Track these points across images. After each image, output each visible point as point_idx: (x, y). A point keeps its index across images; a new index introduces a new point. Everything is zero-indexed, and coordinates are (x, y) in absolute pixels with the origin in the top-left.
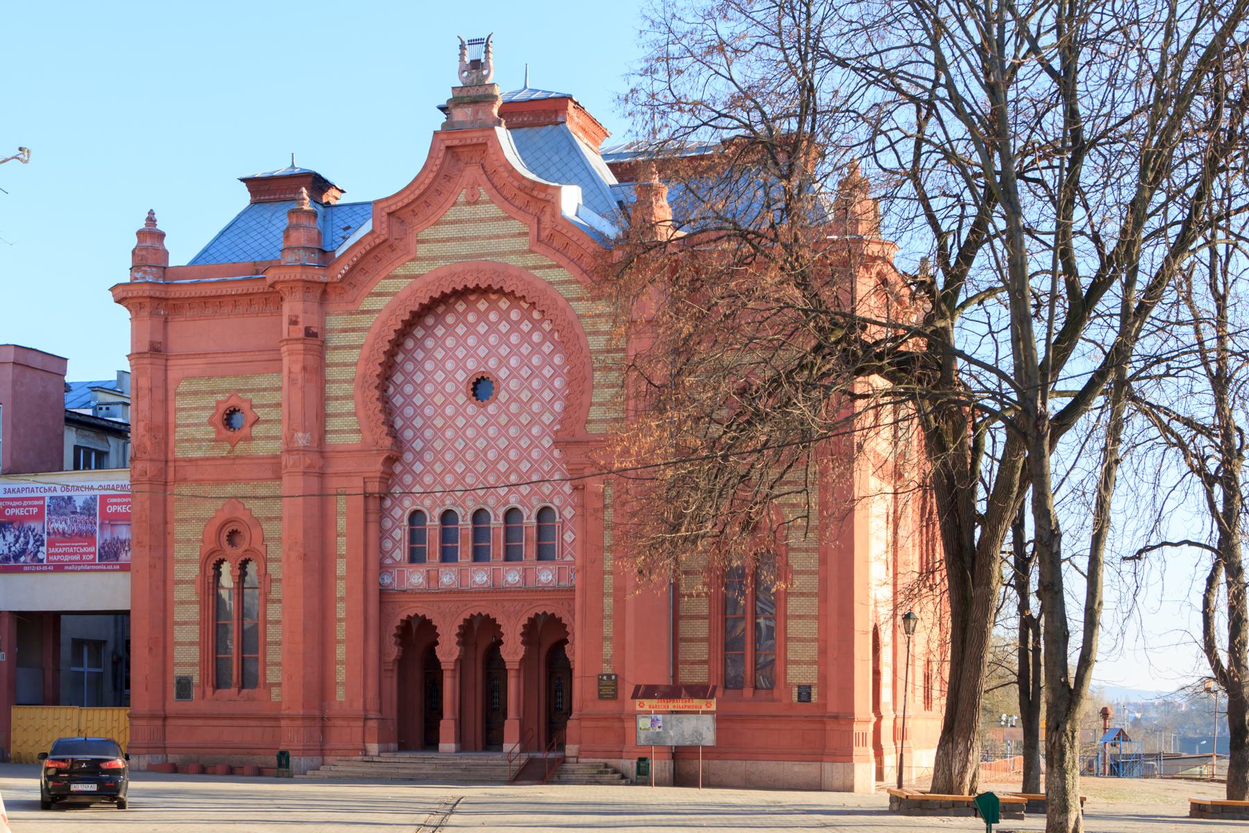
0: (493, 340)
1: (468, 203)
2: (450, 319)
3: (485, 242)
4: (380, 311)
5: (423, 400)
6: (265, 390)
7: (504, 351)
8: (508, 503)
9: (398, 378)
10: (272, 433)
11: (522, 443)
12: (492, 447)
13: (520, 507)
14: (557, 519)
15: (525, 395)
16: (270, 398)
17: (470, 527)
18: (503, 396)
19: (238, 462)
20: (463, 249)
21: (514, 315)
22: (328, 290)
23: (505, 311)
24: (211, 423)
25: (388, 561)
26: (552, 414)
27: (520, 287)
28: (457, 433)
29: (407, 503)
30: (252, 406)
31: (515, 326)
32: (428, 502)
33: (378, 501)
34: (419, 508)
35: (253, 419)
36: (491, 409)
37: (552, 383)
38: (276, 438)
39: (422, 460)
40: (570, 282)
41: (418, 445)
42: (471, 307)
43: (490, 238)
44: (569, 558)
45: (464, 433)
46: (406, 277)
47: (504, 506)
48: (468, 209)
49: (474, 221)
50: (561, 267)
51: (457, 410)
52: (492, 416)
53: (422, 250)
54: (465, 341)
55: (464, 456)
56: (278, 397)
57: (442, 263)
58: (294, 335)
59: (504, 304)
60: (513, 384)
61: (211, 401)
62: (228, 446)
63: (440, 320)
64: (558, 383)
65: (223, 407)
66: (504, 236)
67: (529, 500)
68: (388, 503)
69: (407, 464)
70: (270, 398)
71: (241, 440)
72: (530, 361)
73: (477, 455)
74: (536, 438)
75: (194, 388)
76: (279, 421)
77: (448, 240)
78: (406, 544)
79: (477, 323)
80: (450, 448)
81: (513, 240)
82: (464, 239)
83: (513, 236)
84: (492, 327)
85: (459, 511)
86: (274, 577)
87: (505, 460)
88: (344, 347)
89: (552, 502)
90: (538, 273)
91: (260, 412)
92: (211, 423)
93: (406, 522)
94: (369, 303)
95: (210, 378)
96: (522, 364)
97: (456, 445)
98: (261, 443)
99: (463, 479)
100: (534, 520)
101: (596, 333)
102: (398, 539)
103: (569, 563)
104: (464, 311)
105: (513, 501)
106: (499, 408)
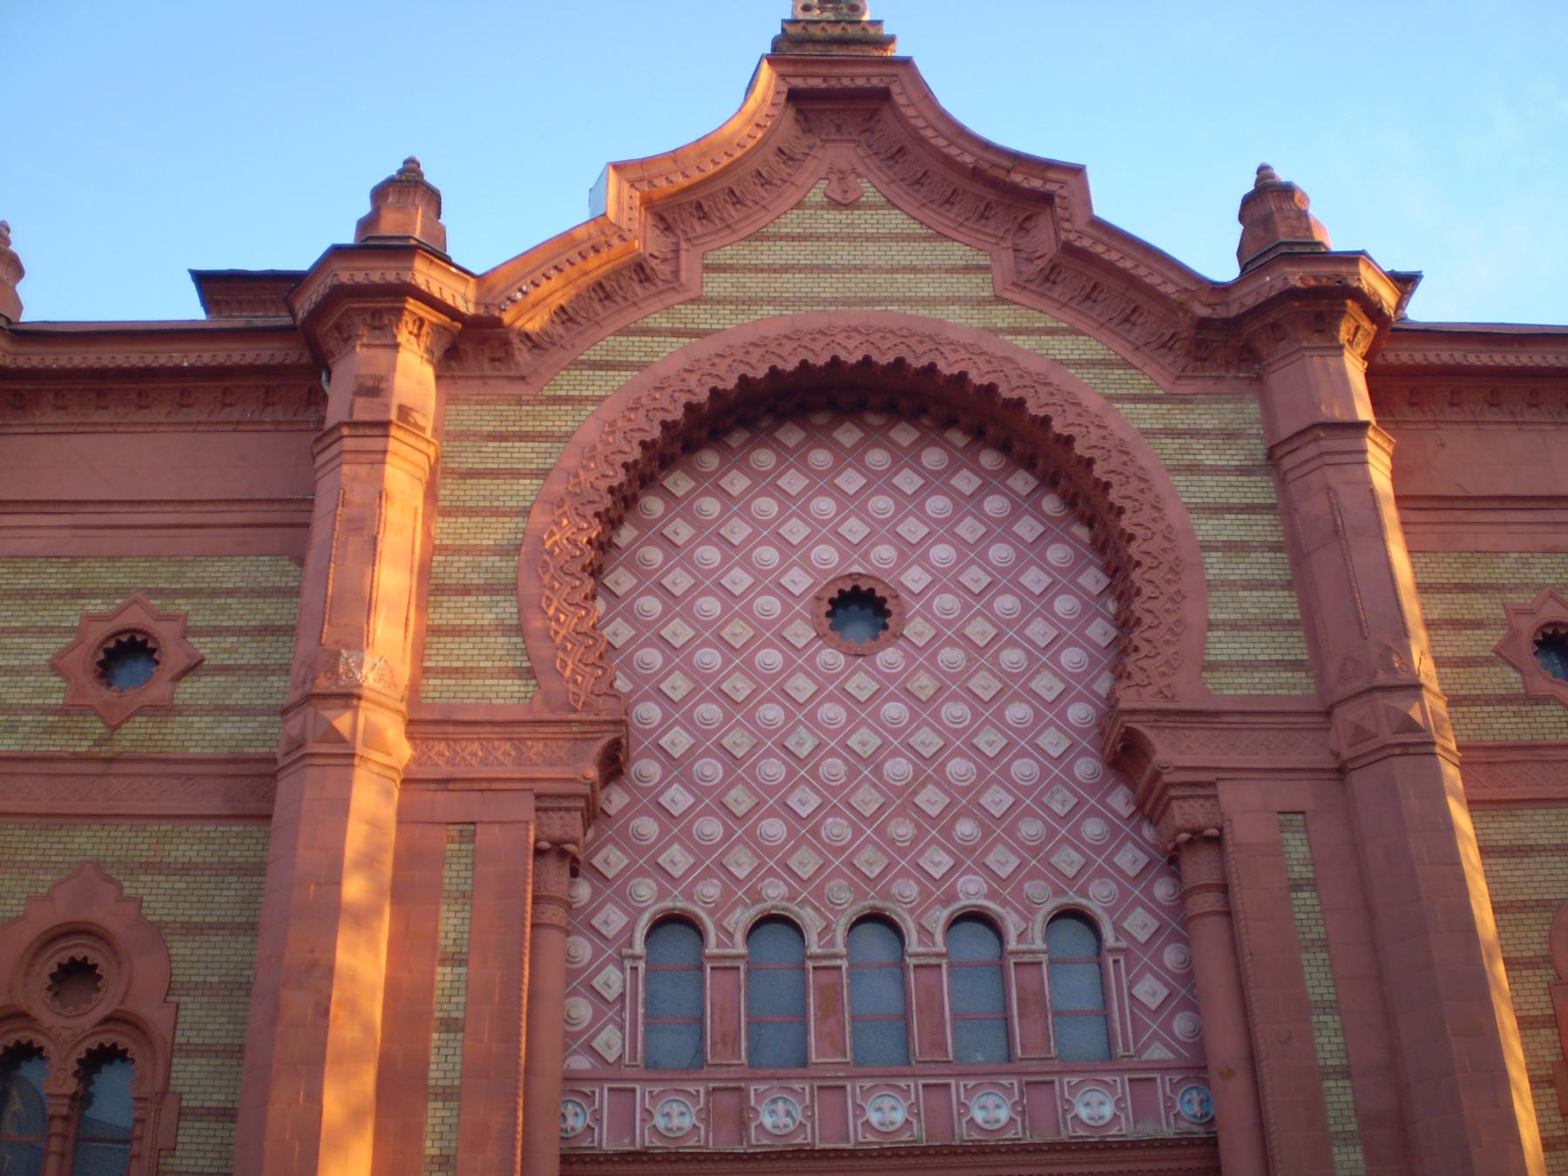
0: (881, 504)
1: (836, 205)
2: (764, 458)
3: (882, 279)
4: (599, 400)
5: (689, 633)
6: (230, 593)
7: (913, 529)
8: (951, 896)
9: (621, 580)
10: (237, 698)
11: (980, 742)
12: (896, 753)
13: (993, 906)
14: (1109, 939)
15: (979, 631)
16: (241, 613)
17: (844, 964)
18: (917, 630)
19: (118, 768)
20: (827, 286)
21: (933, 458)
22: (462, 346)
23: (906, 451)
24: (55, 668)
25: (581, 1063)
26: (1056, 674)
27: (984, 368)
28: (789, 715)
29: (645, 890)
30: (187, 631)
31: (936, 482)
32: (711, 890)
33: (566, 871)
34: (681, 904)
35: (184, 663)
36: (890, 656)
37: (1049, 606)
38: (246, 711)
39: (688, 782)
40: (1107, 364)
41: (678, 740)
42: (819, 436)
43: (893, 270)
44: (1157, 1053)
45: (812, 716)
46: (675, 333)
47: (945, 904)
48: (833, 215)
49: (852, 238)
50: (1084, 334)
51: (789, 662)
52: (891, 678)
53: (716, 285)
54: (805, 507)
55: (814, 772)
56: (271, 611)
57: (769, 311)
58: (359, 416)
59: (904, 435)
60: (947, 603)
61: (70, 615)
62: (98, 728)
63: (735, 459)
64: (1064, 605)
65: (106, 629)
66: (929, 270)
67: (1017, 893)
68: (583, 891)
69: (645, 792)
70: (241, 613)
71: (140, 711)
72: (983, 555)
73: (853, 773)
74: (1023, 733)
75: (24, 582)
76: (264, 670)
77: (785, 269)
78: (641, 1010)
79: (837, 468)
80: (769, 754)
81: (952, 278)
82: (827, 269)
83: (953, 270)
84: (878, 482)
85: (809, 918)
86: (189, 1102)
88: (494, 474)
89: (1088, 898)
90: (1022, 342)
91: (205, 647)
92: (55, 668)
93: (639, 947)
94: (567, 383)
95: (74, 559)
96: (962, 562)
97: (791, 743)
98: (198, 722)
99: (815, 832)
100: (1039, 944)
101: (1194, 469)
102: (611, 995)
103: (1164, 1068)
104: (799, 445)
105: (972, 891)
106: (909, 659)
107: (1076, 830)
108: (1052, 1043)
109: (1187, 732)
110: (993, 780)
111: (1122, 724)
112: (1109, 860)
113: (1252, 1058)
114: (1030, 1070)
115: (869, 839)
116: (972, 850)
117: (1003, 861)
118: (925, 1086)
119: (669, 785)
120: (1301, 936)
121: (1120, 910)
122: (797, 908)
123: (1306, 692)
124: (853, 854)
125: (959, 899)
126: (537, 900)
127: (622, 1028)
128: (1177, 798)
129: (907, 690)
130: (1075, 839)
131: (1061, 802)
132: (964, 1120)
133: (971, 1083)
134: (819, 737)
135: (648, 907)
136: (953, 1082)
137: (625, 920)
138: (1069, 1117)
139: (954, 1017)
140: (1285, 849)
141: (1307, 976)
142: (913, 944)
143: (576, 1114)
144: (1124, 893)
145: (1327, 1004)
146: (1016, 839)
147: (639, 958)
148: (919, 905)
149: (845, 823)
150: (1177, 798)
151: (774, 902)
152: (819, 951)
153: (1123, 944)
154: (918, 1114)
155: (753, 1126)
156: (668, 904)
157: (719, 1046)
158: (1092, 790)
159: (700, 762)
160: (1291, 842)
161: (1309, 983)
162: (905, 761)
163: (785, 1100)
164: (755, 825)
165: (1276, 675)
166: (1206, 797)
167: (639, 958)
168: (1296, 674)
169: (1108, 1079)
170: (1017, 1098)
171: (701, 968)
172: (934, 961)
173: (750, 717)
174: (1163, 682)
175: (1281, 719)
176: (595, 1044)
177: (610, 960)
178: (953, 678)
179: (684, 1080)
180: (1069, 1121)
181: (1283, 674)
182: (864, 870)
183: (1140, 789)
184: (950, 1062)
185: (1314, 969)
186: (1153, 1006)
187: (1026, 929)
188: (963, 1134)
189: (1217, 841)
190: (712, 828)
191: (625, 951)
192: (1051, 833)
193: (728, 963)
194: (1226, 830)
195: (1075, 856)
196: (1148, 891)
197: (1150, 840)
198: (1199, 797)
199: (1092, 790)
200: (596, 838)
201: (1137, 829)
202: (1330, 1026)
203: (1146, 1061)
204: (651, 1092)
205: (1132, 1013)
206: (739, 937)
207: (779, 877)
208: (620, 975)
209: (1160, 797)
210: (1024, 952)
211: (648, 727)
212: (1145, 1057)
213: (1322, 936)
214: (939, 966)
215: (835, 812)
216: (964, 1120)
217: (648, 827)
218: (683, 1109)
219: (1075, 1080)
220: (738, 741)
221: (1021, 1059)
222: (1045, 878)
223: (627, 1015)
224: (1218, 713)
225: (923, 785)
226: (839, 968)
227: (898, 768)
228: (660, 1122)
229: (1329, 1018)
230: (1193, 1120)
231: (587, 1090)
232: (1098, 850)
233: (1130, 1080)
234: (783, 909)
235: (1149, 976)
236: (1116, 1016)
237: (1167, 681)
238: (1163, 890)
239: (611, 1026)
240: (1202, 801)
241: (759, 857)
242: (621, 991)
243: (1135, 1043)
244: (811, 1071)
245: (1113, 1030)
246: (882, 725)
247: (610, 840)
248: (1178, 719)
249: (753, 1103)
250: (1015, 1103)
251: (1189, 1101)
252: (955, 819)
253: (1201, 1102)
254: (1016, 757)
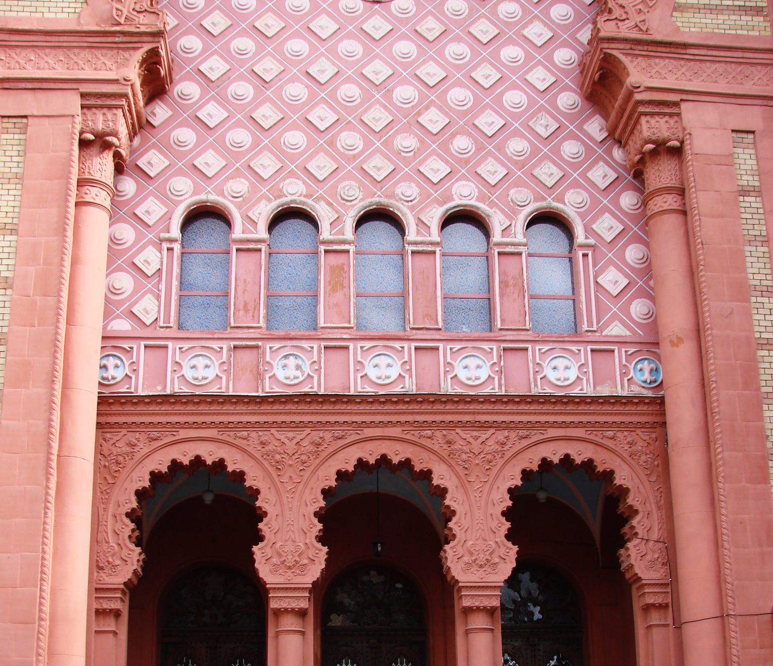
8: (448, 198)
11: (477, 75)
13: (483, 208)
25: (121, 325)
32: (240, 186)
39: (222, 100)
41: (215, 67)
44: (616, 330)
47: (442, 206)
55: (333, 94)
73: (367, 97)
78: (175, 283)
85: (323, 213)
87: (440, 108)
93: (175, 232)
97: (313, 71)
99: (331, 143)
107: (556, 150)
108: (527, 318)
109: (657, 60)
110: (487, 106)
111: (601, 49)
112: (584, 175)
113: (698, 332)
114: (508, 338)
115: (377, 150)
116: (467, 162)
117: (492, 170)
118: (416, 348)
119: (207, 102)
120: (745, 232)
121: (591, 214)
122: (313, 203)
123: (763, 33)
124: (364, 161)
125: (454, 200)
126: (81, 183)
127: (158, 298)
128: (646, 114)
129: (416, 31)
130: (555, 156)
131: (544, 125)
132: (449, 377)
133: (457, 346)
134: (338, 66)
135: (185, 200)
136: (441, 345)
137: (165, 210)
138: (539, 377)
139: (445, 298)
140: (736, 161)
141: (749, 265)
142: (412, 234)
143: (117, 366)
144: (595, 202)
145: (765, 289)
146: (505, 155)
147: (176, 241)
148: (419, 203)
149: (358, 136)
150: (646, 114)
151: (293, 198)
152: (331, 237)
153: (592, 241)
154: (410, 370)
155: (267, 376)
156: (203, 197)
157: (242, 313)
158: (571, 118)
159: (234, 84)
160: (741, 156)
161: (750, 270)
162: (412, 88)
163: (296, 356)
164: (280, 135)
165: (738, 18)
166: (671, 115)
167: (176, 241)
168: (755, 18)
169: (574, 348)
170: (495, 360)
171: (228, 253)
172: (430, 248)
173: (279, 50)
174: (638, 19)
175: (740, 54)
176: (134, 310)
177: (150, 242)
178: (458, 23)
179: (210, 339)
180: (539, 380)
181: (743, 18)
182: (372, 173)
183: (613, 115)
184: (440, 329)
185: (755, 260)
186: (615, 293)
187: (511, 225)
188: (448, 388)
189: (677, 152)
190: (241, 136)
191: (167, 235)
192: (535, 151)
193: (251, 246)
194: (687, 142)
195: (554, 169)
196: (615, 202)
197: (620, 161)
198: (665, 114)
199: (571, 118)
200: (142, 144)
201: (609, 152)
202: (766, 306)
203: (606, 336)
204: (180, 348)
205: (597, 297)
206: (263, 226)
207: (298, 178)
208: (159, 255)
209: (630, 118)
210: (507, 244)
211: (190, 56)
212: (604, 334)
213: (764, 233)
214: (434, 253)
215: (349, 126)
216: (449, 377)
217: (186, 135)
218: (208, 362)
219: (546, 348)
220: (268, 68)
221: (501, 329)
222: (527, 186)
223: (163, 286)
224: (685, 46)
225: (427, 108)
226: (348, 252)
227: (405, 93)
228: (189, 374)
229: (765, 300)
230: (643, 385)
231: (126, 346)
232: (575, 166)
233: (592, 351)
234: (300, 203)
235: (612, 268)
236: (583, 299)
237: (643, 18)
238: (628, 200)
239: (149, 296)
240: (667, 118)
241: (281, 161)
242: (158, 267)
243: (598, 323)
244: (319, 334)
245: (581, 310)
246: (393, 59)
247: (154, 146)
248: (650, 48)
249: (268, 359)
250: (494, 364)
251: (641, 370)
252: (453, 136)
253: (651, 370)
254: (507, 89)
